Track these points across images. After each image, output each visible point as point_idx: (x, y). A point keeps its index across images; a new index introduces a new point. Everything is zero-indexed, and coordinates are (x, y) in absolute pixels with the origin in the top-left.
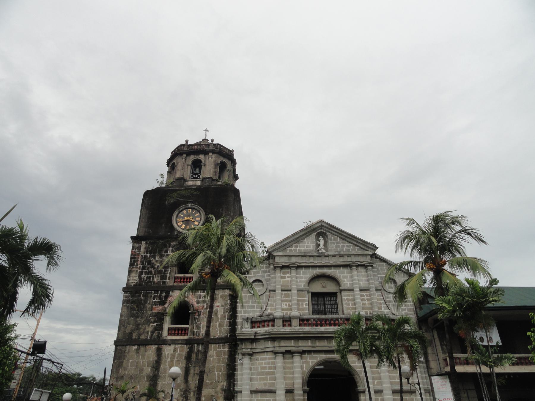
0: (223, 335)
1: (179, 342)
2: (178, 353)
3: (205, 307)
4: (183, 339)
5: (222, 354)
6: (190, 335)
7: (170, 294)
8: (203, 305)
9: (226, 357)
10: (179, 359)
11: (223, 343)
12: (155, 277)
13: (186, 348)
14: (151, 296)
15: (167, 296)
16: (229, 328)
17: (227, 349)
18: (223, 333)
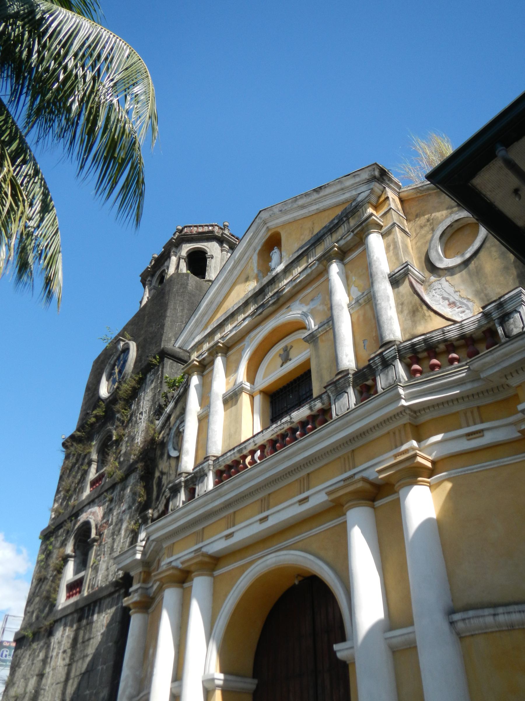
1: (69, 611)
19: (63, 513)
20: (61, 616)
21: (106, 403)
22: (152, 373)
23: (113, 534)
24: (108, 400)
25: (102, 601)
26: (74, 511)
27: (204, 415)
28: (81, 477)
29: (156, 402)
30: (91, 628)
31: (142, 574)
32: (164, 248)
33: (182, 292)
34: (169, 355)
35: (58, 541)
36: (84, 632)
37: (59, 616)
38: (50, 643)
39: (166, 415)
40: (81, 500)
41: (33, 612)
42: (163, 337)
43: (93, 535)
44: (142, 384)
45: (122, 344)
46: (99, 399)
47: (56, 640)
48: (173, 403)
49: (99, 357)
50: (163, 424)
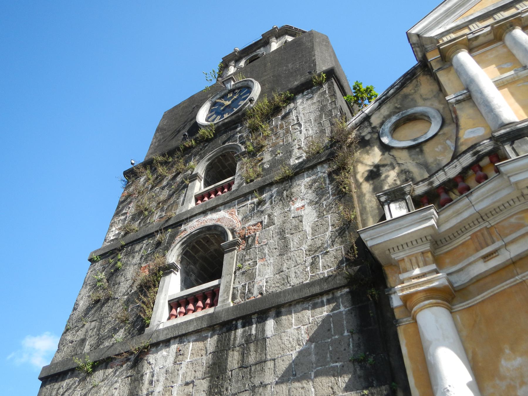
0: (326, 271)
1: (191, 329)
2: (188, 360)
3: (266, 221)
4: (203, 316)
5: (329, 330)
6: (224, 301)
7: (181, 229)
8: (260, 220)
9: (346, 333)
10: (188, 380)
11: (327, 292)
12: (157, 213)
13: (211, 343)
14: (141, 248)
15: (173, 237)
16: (342, 247)
17: (345, 307)
18: (324, 267)
19: (137, 231)
20: (169, 337)
21: (216, 126)
22: (305, 93)
23: (282, 233)
24: (220, 123)
25: (283, 310)
26: (171, 222)
27: (507, 81)
28: (170, 196)
29: (331, 111)
30: (264, 348)
31: (429, 255)
32: (262, 35)
33: (326, 44)
34: (336, 77)
35: (133, 257)
36: (243, 354)
37: (162, 338)
38: (142, 376)
39: (363, 115)
40: (184, 210)
41: (83, 341)
42: (317, 68)
43: (231, 238)
44: (290, 103)
45: (233, 83)
46: (196, 127)
47: (157, 369)
48: (377, 104)
49: (176, 107)
50: (356, 124)
